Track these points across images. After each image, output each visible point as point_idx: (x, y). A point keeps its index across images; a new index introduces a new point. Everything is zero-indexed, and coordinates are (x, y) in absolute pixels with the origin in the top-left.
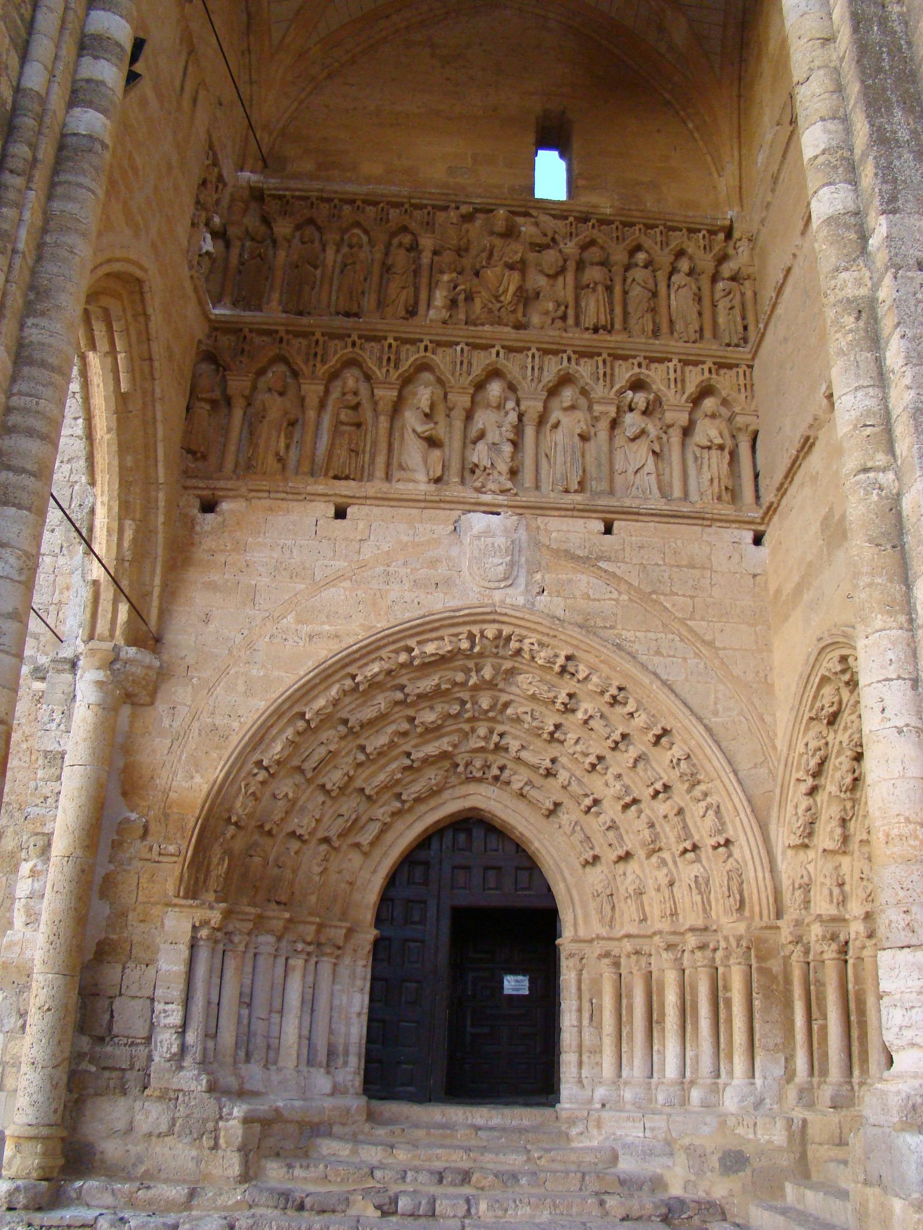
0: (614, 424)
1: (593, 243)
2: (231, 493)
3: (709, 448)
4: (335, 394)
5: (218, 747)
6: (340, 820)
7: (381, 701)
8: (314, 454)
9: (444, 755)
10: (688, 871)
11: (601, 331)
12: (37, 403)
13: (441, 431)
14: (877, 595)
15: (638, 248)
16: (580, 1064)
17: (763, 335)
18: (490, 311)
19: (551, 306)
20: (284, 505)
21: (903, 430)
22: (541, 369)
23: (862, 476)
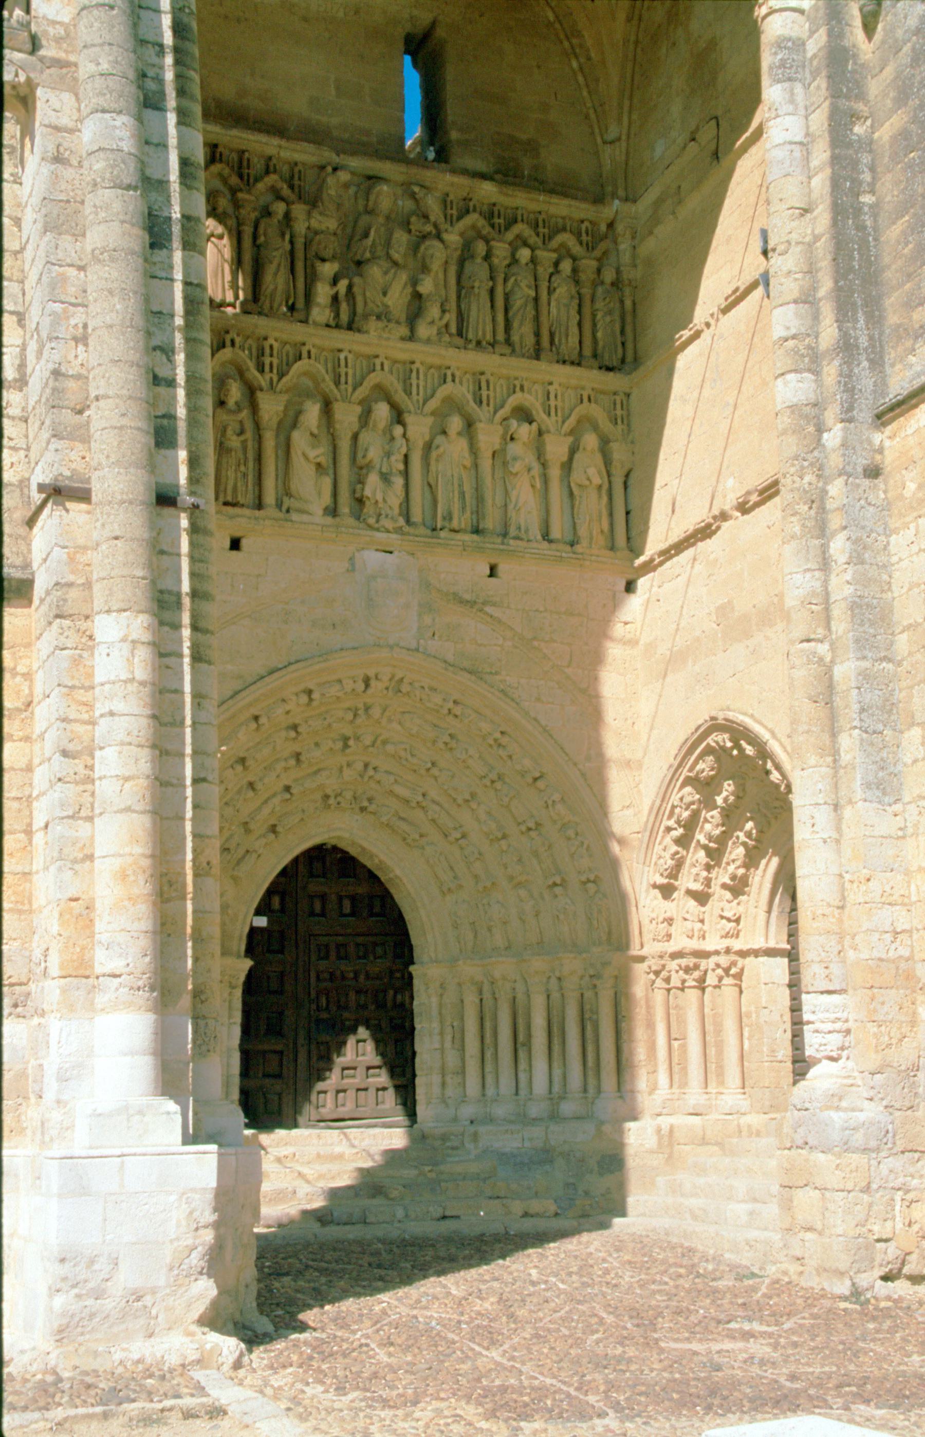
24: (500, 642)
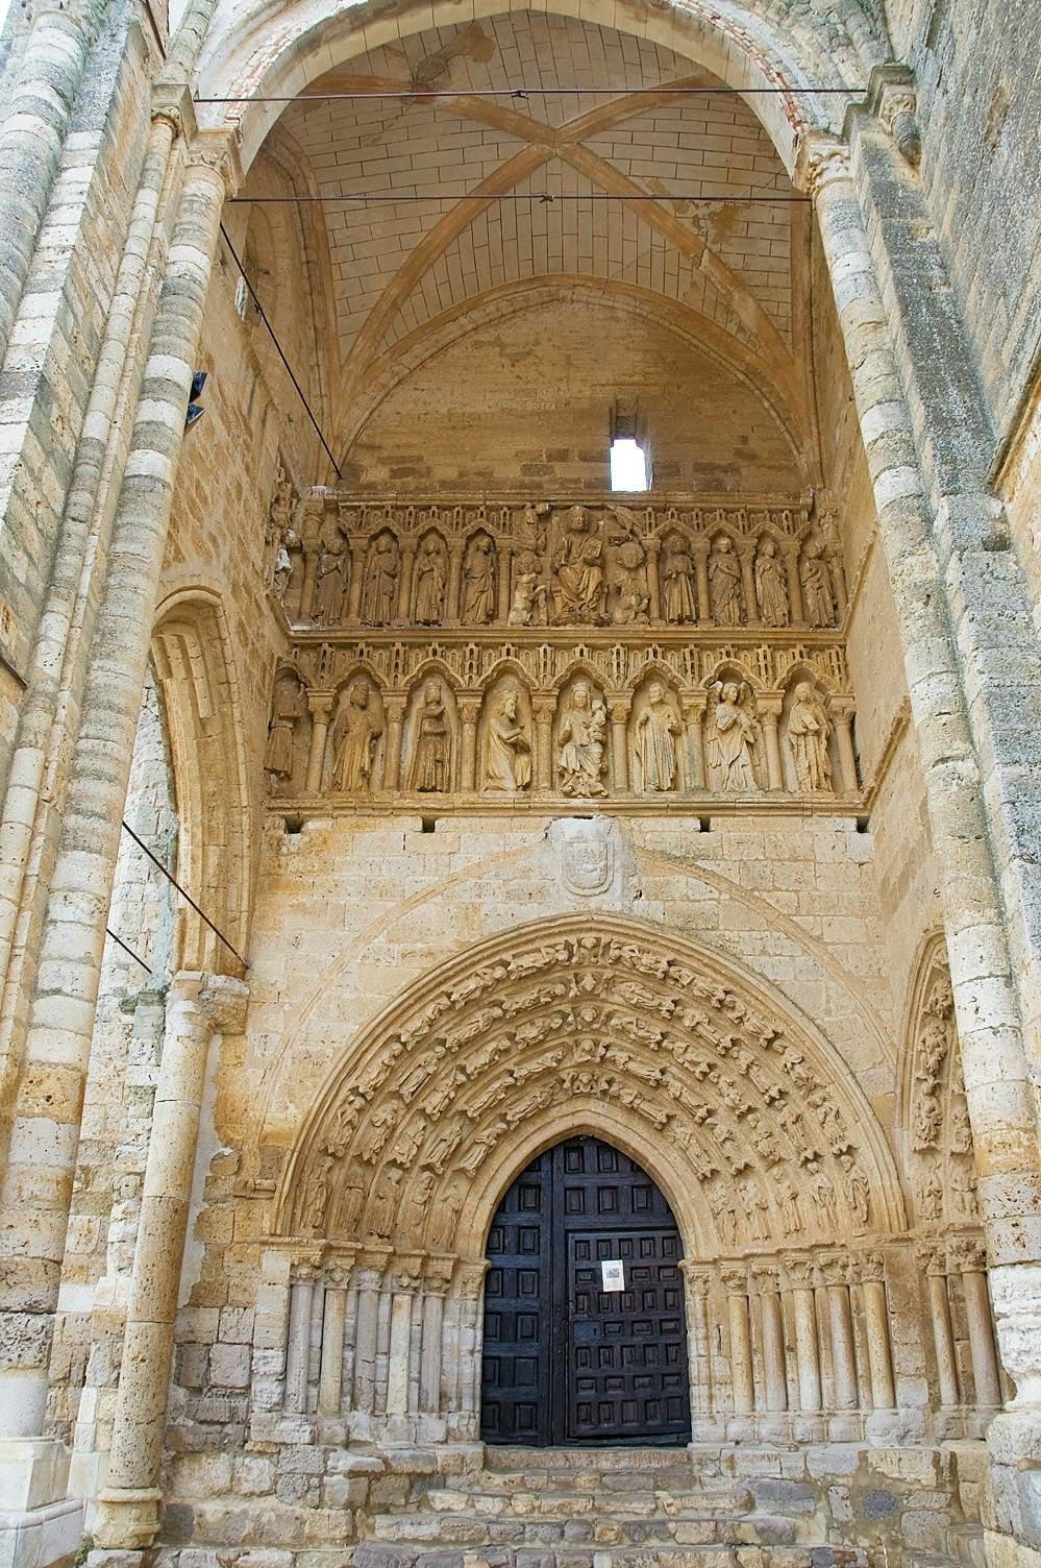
0: (705, 716)
1: (673, 531)
2: (316, 813)
3: (805, 734)
4: (419, 703)
5: (313, 1075)
6: (443, 1145)
7: (479, 1019)
8: (399, 767)
9: (549, 1071)
10: (809, 1185)
11: (686, 622)
12: (105, 745)
13: (527, 735)
14: (963, 890)
15: (720, 533)
16: (711, 1397)
17: (852, 614)
18: (571, 610)
19: (633, 600)
20: (371, 821)
21: (978, 714)
22: (627, 665)
23: (941, 766)
24: (716, 895)
